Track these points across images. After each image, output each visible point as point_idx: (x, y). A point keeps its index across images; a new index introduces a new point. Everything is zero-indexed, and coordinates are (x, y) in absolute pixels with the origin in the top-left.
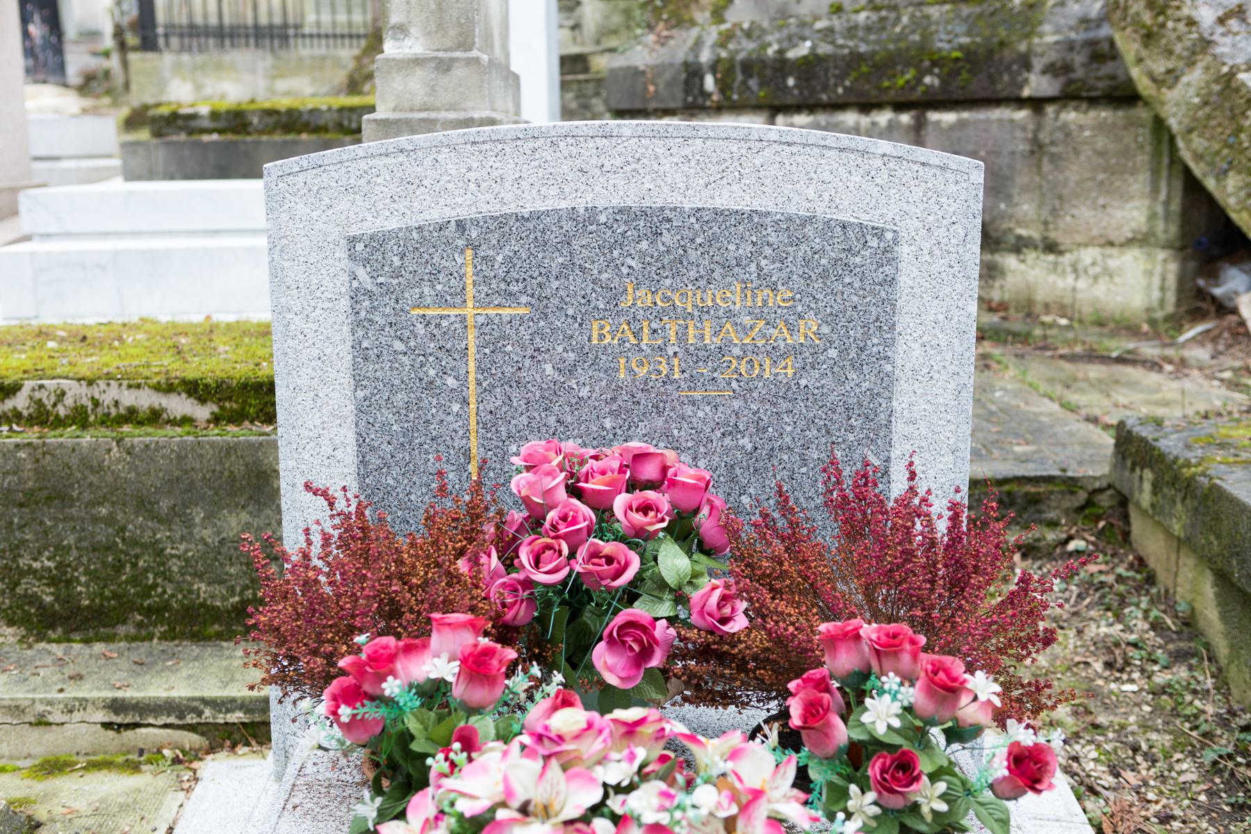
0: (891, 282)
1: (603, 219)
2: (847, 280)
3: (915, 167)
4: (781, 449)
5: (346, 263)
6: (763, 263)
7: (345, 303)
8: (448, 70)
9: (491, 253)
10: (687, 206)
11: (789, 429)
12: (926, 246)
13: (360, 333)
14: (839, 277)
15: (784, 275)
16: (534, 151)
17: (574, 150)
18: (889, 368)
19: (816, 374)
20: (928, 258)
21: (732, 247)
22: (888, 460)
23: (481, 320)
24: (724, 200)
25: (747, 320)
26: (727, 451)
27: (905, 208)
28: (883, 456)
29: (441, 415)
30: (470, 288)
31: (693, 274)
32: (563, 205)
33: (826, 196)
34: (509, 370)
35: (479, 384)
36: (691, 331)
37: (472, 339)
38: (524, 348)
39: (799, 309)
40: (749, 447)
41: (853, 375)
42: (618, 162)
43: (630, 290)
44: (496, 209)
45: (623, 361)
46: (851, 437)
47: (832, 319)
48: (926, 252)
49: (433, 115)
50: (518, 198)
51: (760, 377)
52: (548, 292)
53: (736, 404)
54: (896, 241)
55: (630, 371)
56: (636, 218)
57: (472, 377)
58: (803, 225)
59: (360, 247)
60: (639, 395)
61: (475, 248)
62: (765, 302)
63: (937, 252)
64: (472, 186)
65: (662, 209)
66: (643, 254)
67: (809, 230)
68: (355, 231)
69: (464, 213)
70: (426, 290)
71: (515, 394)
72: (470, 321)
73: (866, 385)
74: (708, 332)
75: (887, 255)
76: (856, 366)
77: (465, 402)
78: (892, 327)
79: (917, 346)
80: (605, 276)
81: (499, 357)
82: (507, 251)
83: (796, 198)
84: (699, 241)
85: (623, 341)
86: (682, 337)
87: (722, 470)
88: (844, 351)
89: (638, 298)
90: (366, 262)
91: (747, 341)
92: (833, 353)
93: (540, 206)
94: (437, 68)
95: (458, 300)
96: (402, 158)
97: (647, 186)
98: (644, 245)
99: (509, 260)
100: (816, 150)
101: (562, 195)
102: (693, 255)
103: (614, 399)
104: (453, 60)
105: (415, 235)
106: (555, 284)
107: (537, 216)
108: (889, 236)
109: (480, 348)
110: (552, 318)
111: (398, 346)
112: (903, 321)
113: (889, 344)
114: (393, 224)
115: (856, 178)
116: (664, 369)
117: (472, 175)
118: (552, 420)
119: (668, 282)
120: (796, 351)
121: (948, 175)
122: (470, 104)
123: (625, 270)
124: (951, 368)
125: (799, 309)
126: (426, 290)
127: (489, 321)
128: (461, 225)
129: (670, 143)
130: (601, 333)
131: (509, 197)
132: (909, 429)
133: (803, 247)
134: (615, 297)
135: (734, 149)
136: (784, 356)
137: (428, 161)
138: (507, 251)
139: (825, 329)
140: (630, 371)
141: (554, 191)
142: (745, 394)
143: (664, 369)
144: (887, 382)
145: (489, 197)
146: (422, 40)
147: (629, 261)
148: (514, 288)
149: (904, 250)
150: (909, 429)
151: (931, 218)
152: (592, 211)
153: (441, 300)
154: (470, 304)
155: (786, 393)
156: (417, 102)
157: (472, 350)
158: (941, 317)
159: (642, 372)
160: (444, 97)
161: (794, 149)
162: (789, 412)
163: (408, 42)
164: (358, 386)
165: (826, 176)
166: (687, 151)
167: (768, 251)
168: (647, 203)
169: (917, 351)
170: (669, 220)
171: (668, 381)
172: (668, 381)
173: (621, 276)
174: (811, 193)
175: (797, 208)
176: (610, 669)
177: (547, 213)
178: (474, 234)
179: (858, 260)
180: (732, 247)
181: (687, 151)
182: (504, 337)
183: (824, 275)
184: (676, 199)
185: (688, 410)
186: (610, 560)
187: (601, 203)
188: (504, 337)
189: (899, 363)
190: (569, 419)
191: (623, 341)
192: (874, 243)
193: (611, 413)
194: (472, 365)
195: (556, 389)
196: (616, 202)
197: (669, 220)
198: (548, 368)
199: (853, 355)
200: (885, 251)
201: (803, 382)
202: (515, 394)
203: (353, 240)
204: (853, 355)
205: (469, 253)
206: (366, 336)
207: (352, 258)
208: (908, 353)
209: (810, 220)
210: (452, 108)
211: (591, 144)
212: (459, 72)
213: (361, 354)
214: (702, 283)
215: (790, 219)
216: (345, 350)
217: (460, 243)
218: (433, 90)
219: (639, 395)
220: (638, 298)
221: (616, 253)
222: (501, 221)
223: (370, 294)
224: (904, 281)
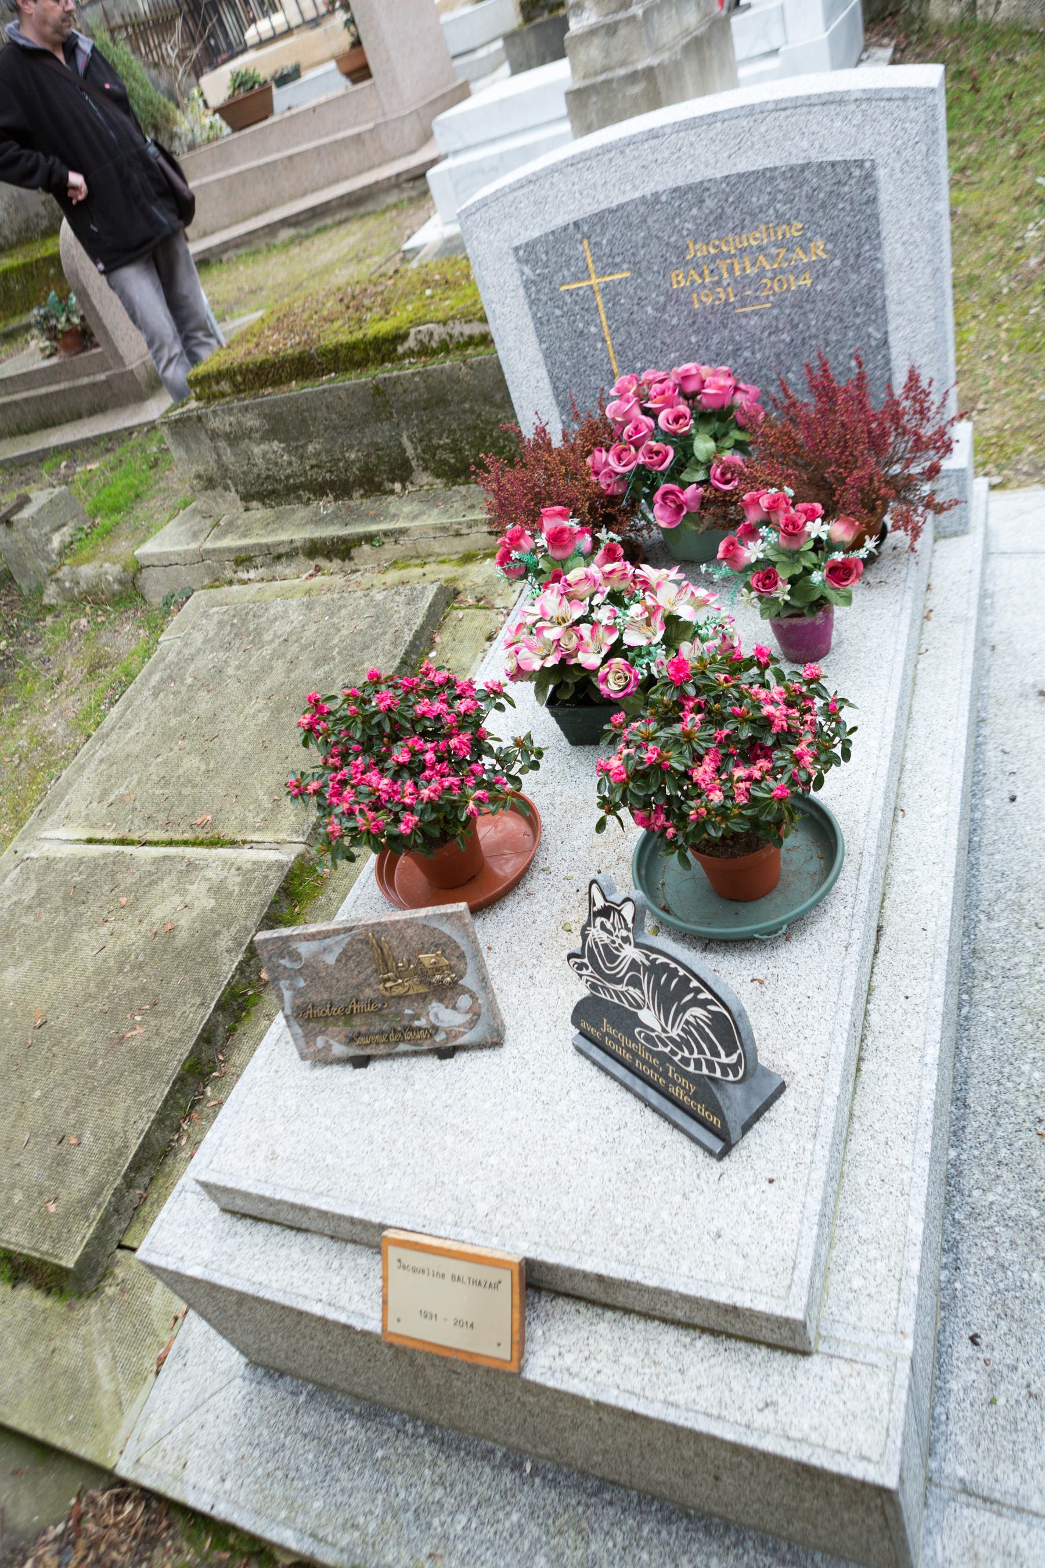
0: (873, 200)
1: (664, 198)
2: (841, 206)
3: (882, 104)
4: (810, 337)
5: (515, 265)
6: (778, 206)
7: (521, 291)
8: (615, 32)
9: (598, 239)
10: (718, 176)
11: (813, 322)
12: (898, 165)
13: (535, 308)
14: (835, 205)
15: (794, 211)
16: (611, 160)
17: (636, 153)
18: (879, 266)
19: (827, 280)
20: (899, 175)
21: (754, 199)
22: (886, 333)
23: (602, 286)
24: (744, 165)
25: (773, 251)
26: (774, 345)
27: (878, 138)
28: (883, 330)
29: (592, 352)
30: (591, 266)
31: (730, 225)
32: (637, 195)
33: (817, 144)
34: (626, 315)
35: (610, 327)
36: (737, 267)
37: (599, 299)
38: (632, 299)
39: (809, 235)
40: (788, 339)
41: (854, 277)
42: (667, 154)
43: (691, 246)
44: (595, 208)
45: (695, 296)
46: (858, 321)
47: (832, 238)
48: (897, 171)
49: (609, 75)
50: (607, 197)
51: (788, 290)
52: (638, 258)
53: (775, 312)
54: (873, 168)
55: (700, 301)
56: (685, 193)
57: (604, 324)
58: (802, 171)
59: (521, 253)
60: (710, 317)
61: (589, 238)
62: (784, 235)
63: (907, 169)
64: (577, 195)
65: (702, 182)
66: (695, 218)
67: (807, 174)
68: (516, 243)
69: (577, 216)
70: (566, 273)
71: (633, 330)
72: (596, 288)
73: (864, 282)
74: (748, 264)
75: (869, 179)
76: (856, 269)
77: (604, 341)
78: (878, 235)
79: (899, 245)
80: (673, 239)
81: (618, 308)
82: (608, 236)
83: (794, 151)
84: (731, 199)
85: (693, 282)
86: (731, 270)
87: (772, 358)
88: (845, 260)
89: (697, 251)
90: (527, 262)
91: (775, 266)
92: (837, 263)
93: (623, 200)
94: (607, 33)
95: (586, 275)
96: (531, 187)
97: (690, 167)
98: (694, 211)
99: (610, 242)
100: (804, 109)
101: (635, 187)
102: (729, 211)
103: (694, 323)
104: (617, 23)
105: (551, 238)
106: (642, 252)
107: (621, 207)
108: (868, 164)
109: (606, 304)
110: (645, 275)
111: (558, 312)
112: (887, 229)
113: (878, 248)
114: (536, 234)
115: (838, 124)
116: (722, 296)
117: (576, 187)
118: (658, 343)
119: (715, 234)
120: (810, 265)
121: (909, 103)
122: (635, 57)
123: (685, 233)
124: (927, 257)
125: (809, 235)
126: (566, 273)
127: (607, 285)
128: (576, 224)
129: (699, 130)
130: (679, 280)
131: (601, 197)
132: (899, 308)
133: (805, 188)
134: (682, 251)
135: (745, 123)
136: (803, 272)
137: (547, 185)
138: (608, 236)
139: (830, 246)
140: (700, 301)
141: (629, 187)
142: (779, 305)
143: (722, 296)
144: (879, 278)
145: (590, 200)
146: (595, 10)
147: (687, 225)
148: (618, 260)
149: (881, 173)
150: (899, 308)
151: (899, 142)
152: (656, 196)
153: (576, 279)
154: (593, 276)
155: (806, 298)
156: (598, 67)
157: (601, 307)
158: (915, 220)
159: (709, 301)
160: (616, 56)
161: (788, 112)
162: (812, 311)
163: (585, 15)
164: (541, 342)
165: (815, 128)
166: (712, 134)
167: (780, 196)
168: (691, 180)
169: (900, 250)
170: (708, 189)
171: (727, 303)
172: (727, 303)
173: (683, 237)
174: (805, 144)
175: (798, 160)
176: (662, 518)
177: (627, 204)
178: (586, 229)
179: (846, 189)
180: (754, 199)
181: (712, 134)
182: (618, 294)
183: (823, 206)
184: (709, 173)
185: (744, 321)
186: (657, 453)
187: (661, 188)
188: (618, 294)
189: (887, 261)
190: (668, 341)
191: (693, 282)
192: (857, 173)
193: (694, 332)
194: (603, 317)
195: (656, 325)
196: (671, 185)
197: (708, 189)
198: (649, 309)
199: (852, 261)
200: (866, 178)
201: (819, 288)
202: (633, 330)
203: (516, 249)
204: (852, 261)
205: (585, 242)
206: (538, 310)
207: (519, 260)
208: (893, 250)
209: (804, 167)
210: (623, 64)
211: (646, 146)
212: (623, 32)
213: (539, 323)
214: (738, 230)
215: (792, 169)
216: (529, 321)
217: (579, 236)
218: (607, 53)
219: (710, 317)
220: (697, 251)
221: (677, 221)
222: (600, 216)
223: (534, 282)
224: (884, 198)
